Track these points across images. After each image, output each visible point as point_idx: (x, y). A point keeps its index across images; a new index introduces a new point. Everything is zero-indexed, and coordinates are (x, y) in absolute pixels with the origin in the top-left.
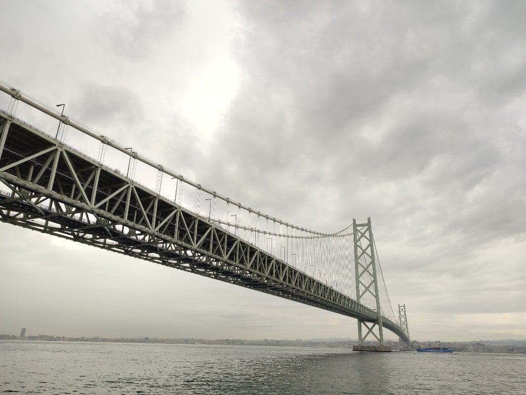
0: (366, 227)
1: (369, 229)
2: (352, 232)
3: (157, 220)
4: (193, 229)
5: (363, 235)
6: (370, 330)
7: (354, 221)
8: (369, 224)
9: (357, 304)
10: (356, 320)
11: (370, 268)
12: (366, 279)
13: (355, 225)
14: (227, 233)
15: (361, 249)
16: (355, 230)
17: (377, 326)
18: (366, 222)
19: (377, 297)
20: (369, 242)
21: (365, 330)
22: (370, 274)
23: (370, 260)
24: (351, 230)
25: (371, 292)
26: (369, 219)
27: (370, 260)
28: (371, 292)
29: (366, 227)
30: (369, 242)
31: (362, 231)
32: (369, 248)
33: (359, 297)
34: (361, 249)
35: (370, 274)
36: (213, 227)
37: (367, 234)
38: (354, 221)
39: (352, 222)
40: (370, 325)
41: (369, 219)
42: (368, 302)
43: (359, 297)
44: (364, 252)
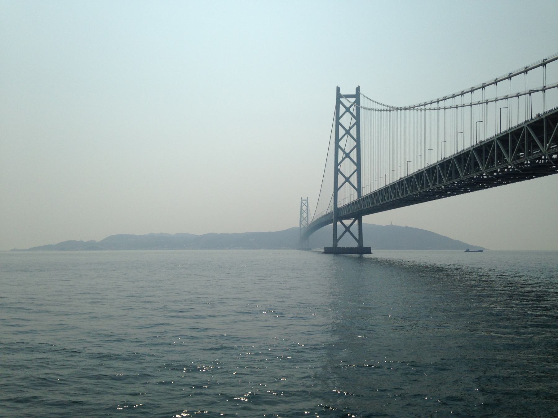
0: (353, 100)
1: (357, 102)
8: (357, 96)
18: (354, 93)
26: (358, 89)
41: (358, 89)
44: (348, 132)
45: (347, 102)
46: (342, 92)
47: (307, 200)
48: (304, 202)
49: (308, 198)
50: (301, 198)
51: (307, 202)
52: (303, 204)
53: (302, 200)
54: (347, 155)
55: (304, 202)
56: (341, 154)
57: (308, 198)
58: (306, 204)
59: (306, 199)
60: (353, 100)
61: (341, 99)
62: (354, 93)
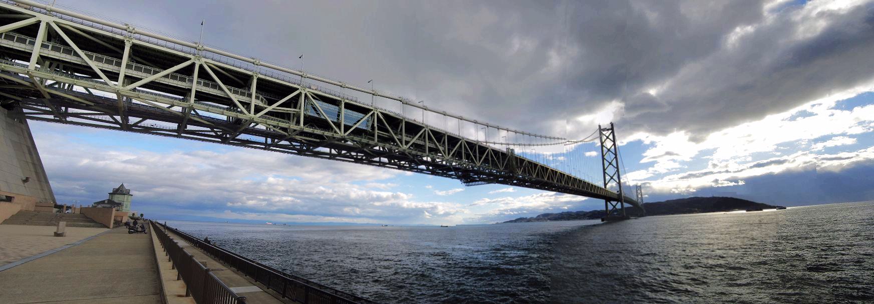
0: (611, 131)
1: (613, 132)
2: (599, 135)
3: (449, 149)
4: (475, 152)
5: (608, 137)
6: (614, 207)
7: (600, 126)
9: (605, 190)
10: (604, 201)
11: (614, 163)
12: (611, 171)
14: (500, 151)
15: (607, 148)
16: (601, 134)
17: (619, 203)
18: (610, 127)
21: (610, 207)
22: (614, 167)
24: (598, 134)
29: (611, 131)
31: (607, 135)
33: (605, 185)
35: (614, 167)
36: (490, 148)
37: (611, 137)
38: (600, 126)
40: (614, 203)
42: (612, 185)
43: (605, 185)
45: (607, 133)
46: (602, 128)
61: (604, 133)
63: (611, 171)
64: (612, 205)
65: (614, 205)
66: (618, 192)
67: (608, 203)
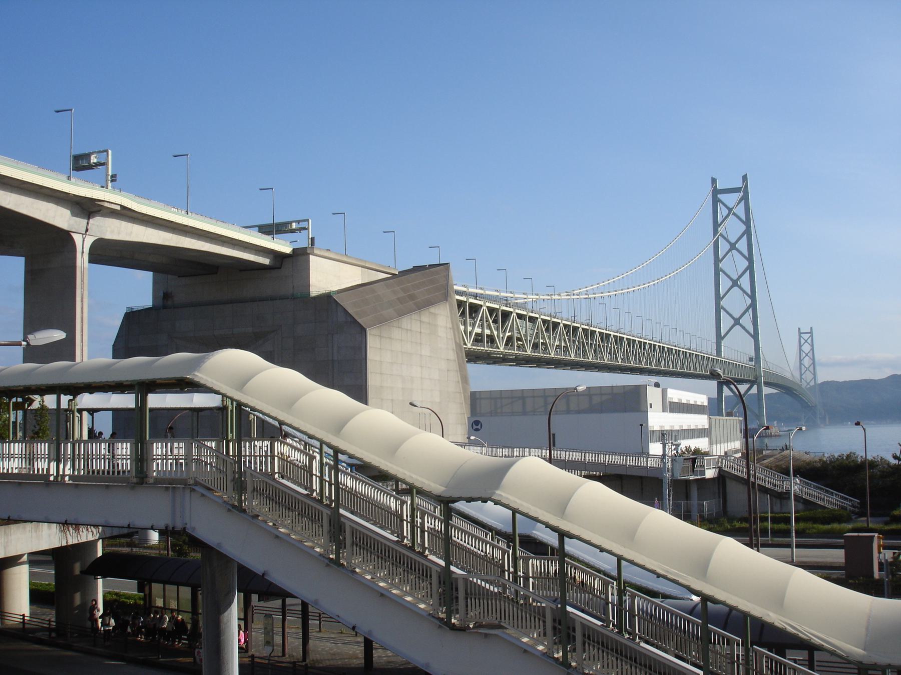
1: (745, 198)
11: (745, 282)
13: (716, 192)
15: (727, 240)
16: (716, 201)
19: (755, 336)
20: (744, 228)
22: (744, 292)
23: (746, 263)
25: (743, 328)
26: (745, 178)
27: (746, 263)
28: (743, 328)
30: (744, 228)
32: (745, 239)
34: (727, 240)
35: (744, 292)
37: (740, 210)
39: (709, 189)
41: (745, 178)
43: (719, 338)
45: (730, 199)
47: (811, 332)
48: (806, 336)
49: (811, 328)
50: (799, 329)
51: (812, 336)
52: (803, 341)
53: (800, 333)
54: (735, 283)
55: (806, 336)
56: (725, 283)
57: (811, 328)
58: (809, 341)
59: (810, 331)
60: (737, 196)
62: (739, 184)
63: (735, 302)
64: (808, 339)
65: (808, 341)
66: (751, 359)
67: (725, 387)
